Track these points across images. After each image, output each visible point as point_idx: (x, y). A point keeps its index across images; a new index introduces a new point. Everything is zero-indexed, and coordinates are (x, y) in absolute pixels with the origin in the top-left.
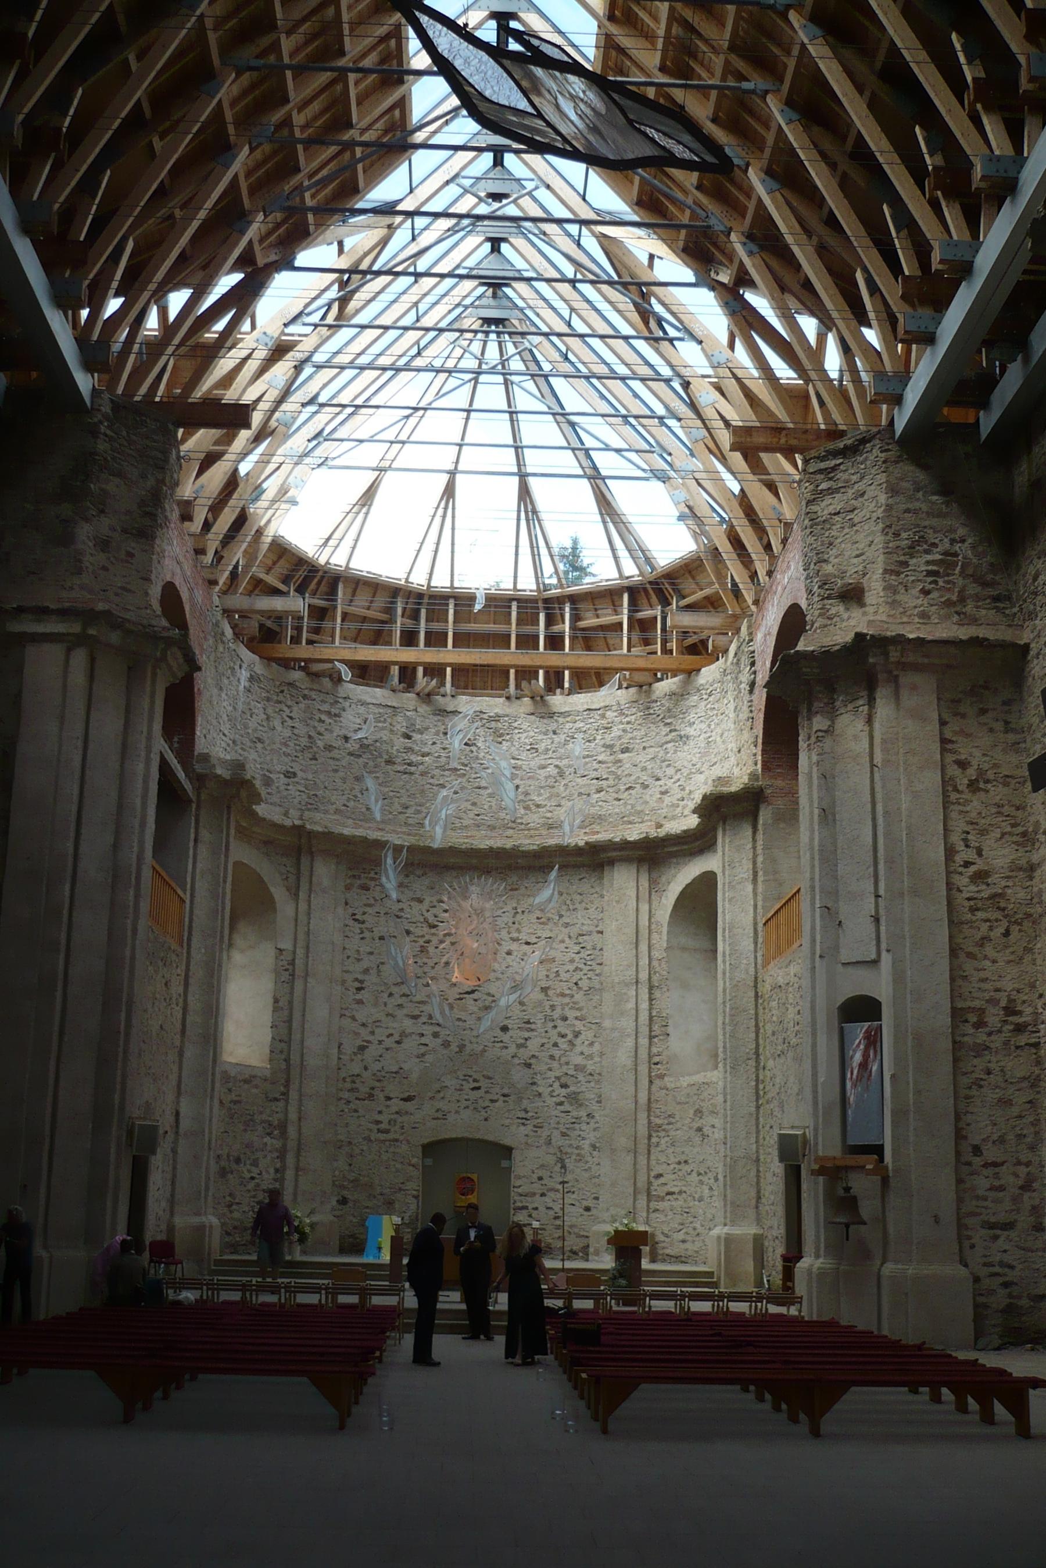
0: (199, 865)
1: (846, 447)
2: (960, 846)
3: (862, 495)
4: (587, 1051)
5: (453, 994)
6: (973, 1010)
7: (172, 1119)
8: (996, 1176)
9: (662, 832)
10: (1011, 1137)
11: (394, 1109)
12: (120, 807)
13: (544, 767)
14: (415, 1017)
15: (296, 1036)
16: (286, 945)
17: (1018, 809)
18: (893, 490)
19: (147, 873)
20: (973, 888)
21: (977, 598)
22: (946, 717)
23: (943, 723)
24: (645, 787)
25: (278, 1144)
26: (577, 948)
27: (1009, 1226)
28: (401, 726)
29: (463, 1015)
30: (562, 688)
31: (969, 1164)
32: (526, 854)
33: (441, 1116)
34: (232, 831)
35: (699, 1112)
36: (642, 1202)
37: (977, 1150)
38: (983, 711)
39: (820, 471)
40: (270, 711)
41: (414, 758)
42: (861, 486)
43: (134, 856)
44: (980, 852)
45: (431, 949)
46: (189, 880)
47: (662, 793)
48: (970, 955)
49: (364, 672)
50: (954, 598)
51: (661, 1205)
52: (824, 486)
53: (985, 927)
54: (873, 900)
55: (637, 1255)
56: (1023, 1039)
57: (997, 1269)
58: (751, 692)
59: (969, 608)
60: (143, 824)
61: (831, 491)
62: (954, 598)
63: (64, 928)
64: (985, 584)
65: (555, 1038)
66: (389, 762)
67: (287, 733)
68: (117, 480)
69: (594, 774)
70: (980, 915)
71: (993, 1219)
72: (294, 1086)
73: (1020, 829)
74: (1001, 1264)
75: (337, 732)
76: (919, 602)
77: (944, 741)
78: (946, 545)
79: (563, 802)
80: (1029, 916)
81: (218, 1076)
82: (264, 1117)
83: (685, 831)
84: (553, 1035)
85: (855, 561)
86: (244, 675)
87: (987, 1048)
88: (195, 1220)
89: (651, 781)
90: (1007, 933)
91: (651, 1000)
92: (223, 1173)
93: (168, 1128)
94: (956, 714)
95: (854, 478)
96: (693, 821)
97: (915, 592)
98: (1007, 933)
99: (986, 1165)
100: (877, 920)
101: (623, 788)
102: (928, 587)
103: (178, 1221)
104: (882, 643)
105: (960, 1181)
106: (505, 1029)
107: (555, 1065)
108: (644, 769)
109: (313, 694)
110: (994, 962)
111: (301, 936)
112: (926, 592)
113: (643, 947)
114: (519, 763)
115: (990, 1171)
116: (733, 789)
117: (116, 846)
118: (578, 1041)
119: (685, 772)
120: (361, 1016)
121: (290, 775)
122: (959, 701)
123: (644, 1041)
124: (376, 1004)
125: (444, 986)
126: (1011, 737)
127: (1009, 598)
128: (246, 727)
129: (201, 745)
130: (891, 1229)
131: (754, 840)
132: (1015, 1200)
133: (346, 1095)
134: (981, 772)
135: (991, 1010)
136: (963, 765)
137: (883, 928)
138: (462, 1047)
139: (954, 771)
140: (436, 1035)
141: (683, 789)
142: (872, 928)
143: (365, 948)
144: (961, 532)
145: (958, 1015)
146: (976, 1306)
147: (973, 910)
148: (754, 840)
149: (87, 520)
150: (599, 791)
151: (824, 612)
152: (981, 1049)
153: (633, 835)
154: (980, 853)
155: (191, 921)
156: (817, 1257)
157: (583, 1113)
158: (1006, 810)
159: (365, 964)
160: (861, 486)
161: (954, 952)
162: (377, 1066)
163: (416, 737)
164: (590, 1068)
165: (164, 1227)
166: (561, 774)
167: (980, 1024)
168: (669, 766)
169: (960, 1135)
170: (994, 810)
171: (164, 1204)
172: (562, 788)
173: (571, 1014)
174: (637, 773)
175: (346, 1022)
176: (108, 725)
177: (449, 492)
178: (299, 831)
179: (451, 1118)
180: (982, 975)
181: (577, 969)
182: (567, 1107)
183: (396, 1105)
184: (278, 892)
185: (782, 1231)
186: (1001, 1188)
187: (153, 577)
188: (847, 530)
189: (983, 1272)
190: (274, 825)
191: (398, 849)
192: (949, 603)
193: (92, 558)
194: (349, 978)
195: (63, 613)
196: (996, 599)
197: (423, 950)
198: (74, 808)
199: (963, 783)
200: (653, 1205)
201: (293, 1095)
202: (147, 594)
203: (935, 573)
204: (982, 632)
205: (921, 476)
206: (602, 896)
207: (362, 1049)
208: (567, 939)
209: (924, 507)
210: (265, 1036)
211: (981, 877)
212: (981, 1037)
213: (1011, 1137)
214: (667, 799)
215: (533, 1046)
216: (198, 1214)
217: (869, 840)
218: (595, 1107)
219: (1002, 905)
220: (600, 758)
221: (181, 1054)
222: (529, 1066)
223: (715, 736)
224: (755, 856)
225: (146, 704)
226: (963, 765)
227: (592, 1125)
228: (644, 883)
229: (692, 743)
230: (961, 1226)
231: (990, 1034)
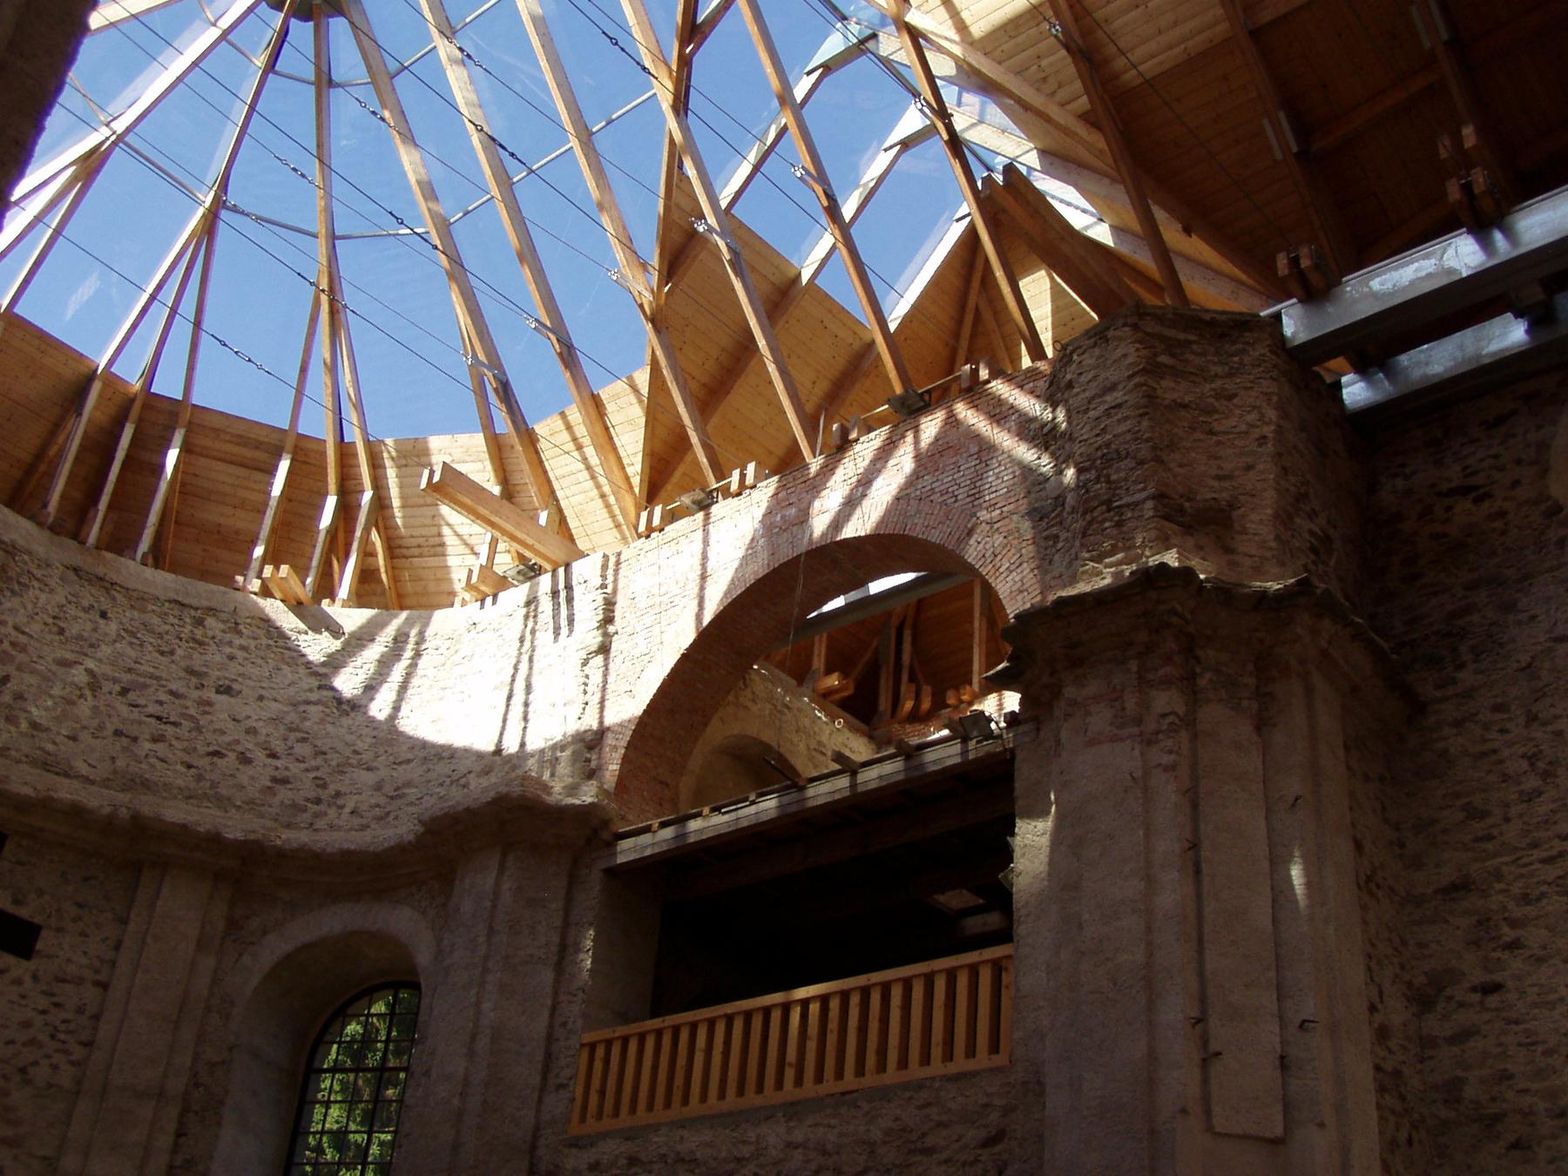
3: (1231, 398)
24: (245, 760)
26: (43, 1002)
47: (274, 780)
69: (152, 709)
79: (85, 736)
83: (347, 854)
85: (1215, 484)
89: (260, 756)
91: (180, 1134)
95: (1219, 370)
101: (202, 749)
108: (251, 731)
114: (23, 639)
141: (324, 786)
150: (155, 740)
168: (304, 740)
172: (88, 712)
174: (234, 733)
181: (32, 1042)
206: (124, 921)
208: (28, 979)
214: (284, 794)
220: (173, 686)
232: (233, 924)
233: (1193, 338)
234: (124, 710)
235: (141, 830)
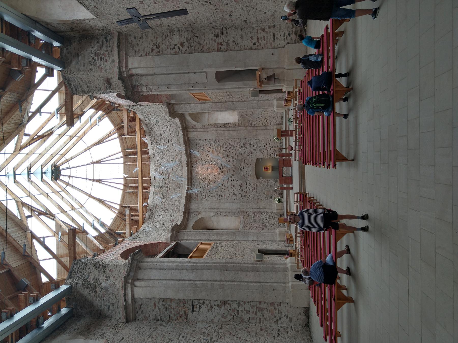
0: (193, 239)
1: (68, 83)
2: (174, 50)
4: (234, 142)
5: (221, 174)
6: (218, 46)
7: (254, 242)
8: (261, 38)
9: (180, 126)
10: (251, 35)
11: (249, 186)
12: (176, 269)
13: (167, 155)
14: (227, 182)
15: (233, 210)
16: (212, 214)
17: (163, 35)
18: (79, 70)
19: (193, 260)
20: (185, 47)
21: (107, 47)
22: (139, 55)
23: (142, 55)
24: (170, 130)
25: (258, 214)
27: (274, 35)
28: (158, 189)
29: (226, 171)
30: (146, 151)
31: (258, 46)
32: (188, 159)
33: (250, 175)
34: (185, 230)
35: (247, 115)
36: (268, 127)
37: (254, 44)
38: (138, 44)
39: (76, 90)
40: (156, 221)
41: (166, 186)
42: (79, 79)
43: (189, 264)
44: (176, 45)
45: (211, 179)
46: (197, 241)
48: (203, 47)
49: (145, 198)
50: (107, 53)
51: (269, 123)
52: (80, 89)
53: (196, 43)
54: (190, 74)
55: (282, 132)
56: (225, 32)
57: (285, 37)
58: (143, 106)
59: (110, 49)
60: (180, 262)
61: (81, 87)
62: (107, 53)
63: (208, 282)
64: (103, 44)
65: (231, 150)
66: (167, 191)
67: (161, 217)
68: (90, 276)
69: (168, 143)
70: (192, 45)
71: (272, 39)
72: (245, 210)
73: (169, 34)
74: (284, 36)
75: (160, 204)
76: (109, 63)
77: (146, 55)
78: (92, 55)
80: (192, 31)
81: (243, 231)
82: (252, 217)
84: (231, 150)
86: (147, 229)
87: (227, 42)
88: (278, 235)
89: (168, 129)
90: (197, 37)
92: (266, 227)
93: (256, 244)
94: (139, 52)
95: (77, 81)
96: (177, 119)
97: (106, 64)
98: (197, 37)
99: (258, 41)
100: (195, 73)
102: (105, 60)
103: (278, 239)
104: (120, 73)
105: (263, 48)
106: (229, 161)
107: (237, 149)
108: (165, 131)
109: (151, 211)
110: (204, 40)
111: (209, 211)
112: (106, 61)
113: (208, 130)
115: (260, 40)
116: (167, 110)
117: (186, 270)
118: (231, 144)
119: (165, 121)
120: (227, 195)
121: (171, 216)
122: (135, 51)
123: (231, 129)
124: (225, 192)
125: (220, 176)
126: (144, 37)
127: (106, 38)
128: (160, 227)
129: (164, 240)
130: (275, 67)
131: (180, 104)
132: (267, 33)
133: (246, 198)
134: (154, 45)
135: (217, 41)
136: (152, 50)
137: (197, 71)
138: (234, 171)
139: (154, 52)
140: (231, 177)
142: (197, 74)
143: (212, 195)
144: (89, 51)
145: (218, 51)
146: (295, 43)
147: (191, 47)
148: (180, 104)
149: (101, 283)
151: (115, 88)
152: (228, 44)
153: (181, 133)
154: (176, 45)
155: (207, 240)
156: (283, 86)
157: (248, 142)
158: (164, 38)
159: (215, 195)
160: (79, 79)
161: (203, 52)
162: (239, 191)
163: (161, 185)
164: (237, 141)
165: (280, 243)
166: (168, 150)
167: (221, 44)
169: (251, 49)
170: (164, 41)
171: (274, 244)
173: (225, 146)
174: (166, 133)
175: (229, 199)
176: (154, 274)
177: (99, 181)
178: (184, 213)
179: (250, 173)
180: (208, 44)
182: (247, 146)
183: (248, 186)
184: (199, 217)
185: (275, 94)
186: (264, 37)
187: (116, 264)
189: (286, 41)
190: (183, 219)
191: (188, 189)
192: (109, 54)
193: (111, 281)
194: (219, 198)
195: (125, 289)
196: (107, 41)
197: (211, 181)
198: (177, 282)
199: (157, 50)
200: (269, 125)
201: (247, 210)
202: (121, 265)
203: (101, 58)
204: (116, 45)
205: (74, 62)
207: (235, 194)
209: (83, 61)
210: (233, 218)
211: (182, 44)
212: (224, 44)
213: (251, 35)
214: (172, 125)
215: (233, 155)
216: (276, 234)
217: (174, 75)
218: (246, 139)
219: (189, 38)
221: (239, 241)
222: (237, 155)
223: (156, 114)
224: (183, 104)
225: (149, 264)
226: (152, 50)
227: (251, 140)
228: (191, 130)
229: (158, 120)
230: (274, 48)
231: (224, 41)
232: (193, 128)
234: (169, 146)
235: (185, 143)
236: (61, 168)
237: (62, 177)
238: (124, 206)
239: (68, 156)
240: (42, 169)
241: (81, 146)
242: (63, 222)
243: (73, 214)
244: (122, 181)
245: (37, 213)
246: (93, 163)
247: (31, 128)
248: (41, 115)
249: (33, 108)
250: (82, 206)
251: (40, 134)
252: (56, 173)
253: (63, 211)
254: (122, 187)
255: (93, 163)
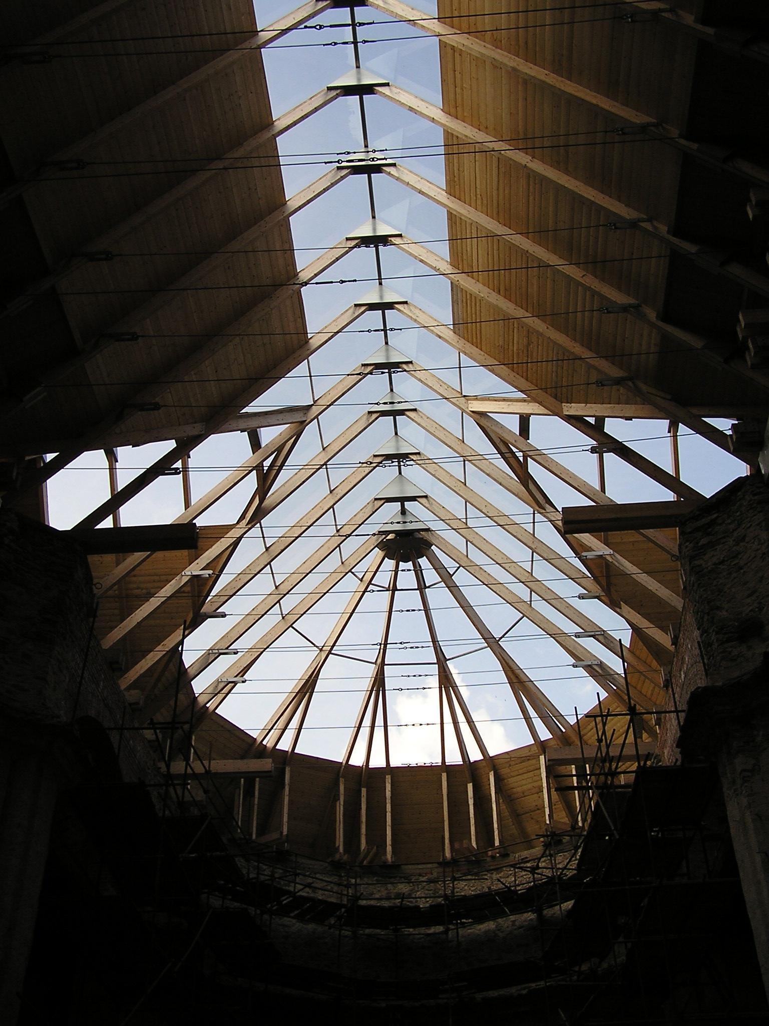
3: (743, 539)
85: (749, 600)
95: (732, 526)
177: (379, 683)
188: (734, 575)
233: (715, 515)
236: (423, 562)
237: (389, 564)
238: (288, 770)
239: (461, 578)
240: (413, 499)
241: (499, 617)
242: (235, 544)
243: (262, 585)
244: (378, 761)
245: (267, 463)
246: (442, 661)
247: (552, 434)
248: (593, 450)
249: (615, 428)
250: (289, 623)
251: (533, 468)
252: (407, 545)
253: (271, 554)
254: (358, 760)
255: (442, 661)
